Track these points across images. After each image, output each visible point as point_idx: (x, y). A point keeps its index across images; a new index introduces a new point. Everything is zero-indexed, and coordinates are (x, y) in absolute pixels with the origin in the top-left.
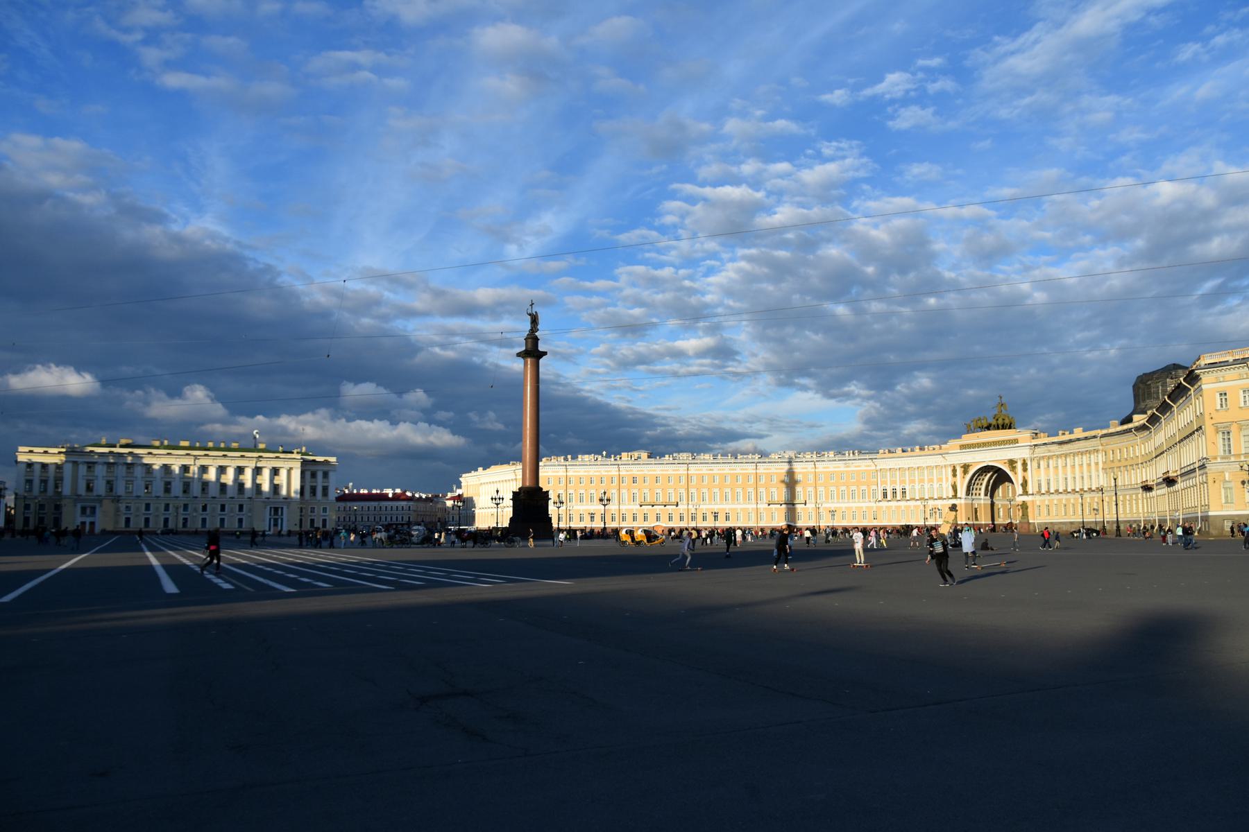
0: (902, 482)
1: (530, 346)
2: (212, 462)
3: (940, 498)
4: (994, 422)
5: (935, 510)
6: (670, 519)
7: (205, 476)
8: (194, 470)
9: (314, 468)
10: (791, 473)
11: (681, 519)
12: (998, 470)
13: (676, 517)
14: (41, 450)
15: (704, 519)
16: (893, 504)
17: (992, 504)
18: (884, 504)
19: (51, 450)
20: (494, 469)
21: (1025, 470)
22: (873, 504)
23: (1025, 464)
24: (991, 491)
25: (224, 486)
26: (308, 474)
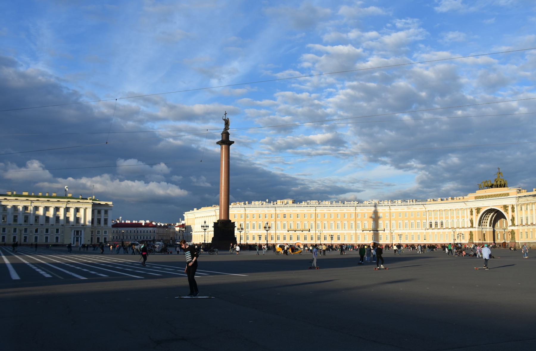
1: (224, 138)
2: (41, 204)
3: (463, 228)
4: (495, 183)
5: (460, 235)
6: (305, 239)
7: (37, 213)
8: (31, 209)
9: (99, 208)
10: (376, 213)
11: (312, 239)
12: (497, 211)
13: (309, 238)
15: (325, 239)
17: (494, 231)
18: (430, 231)
20: (203, 209)
21: (513, 211)
22: (424, 231)
23: (513, 208)
24: (493, 224)
25: (48, 218)
26: (96, 212)
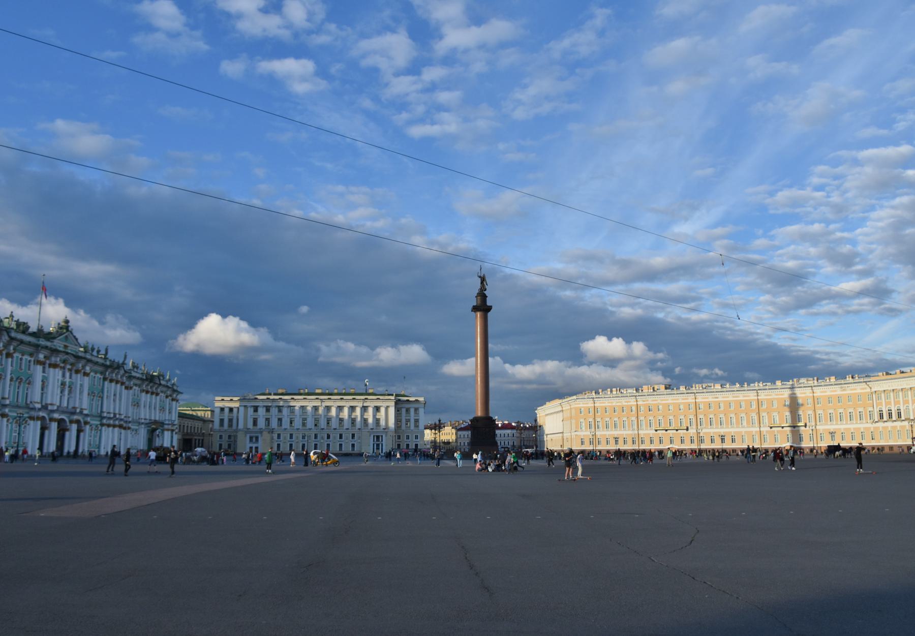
0: (898, 403)
1: (479, 302)
2: (334, 404)
10: (793, 399)
13: (687, 440)
14: (229, 399)
16: (889, 424)
18: (881, 425)
19: (226, 398)
20: (548, 404)
22: (869, 425)
25: (341, 420)
26: (404, 411)
